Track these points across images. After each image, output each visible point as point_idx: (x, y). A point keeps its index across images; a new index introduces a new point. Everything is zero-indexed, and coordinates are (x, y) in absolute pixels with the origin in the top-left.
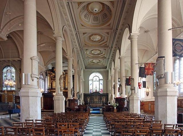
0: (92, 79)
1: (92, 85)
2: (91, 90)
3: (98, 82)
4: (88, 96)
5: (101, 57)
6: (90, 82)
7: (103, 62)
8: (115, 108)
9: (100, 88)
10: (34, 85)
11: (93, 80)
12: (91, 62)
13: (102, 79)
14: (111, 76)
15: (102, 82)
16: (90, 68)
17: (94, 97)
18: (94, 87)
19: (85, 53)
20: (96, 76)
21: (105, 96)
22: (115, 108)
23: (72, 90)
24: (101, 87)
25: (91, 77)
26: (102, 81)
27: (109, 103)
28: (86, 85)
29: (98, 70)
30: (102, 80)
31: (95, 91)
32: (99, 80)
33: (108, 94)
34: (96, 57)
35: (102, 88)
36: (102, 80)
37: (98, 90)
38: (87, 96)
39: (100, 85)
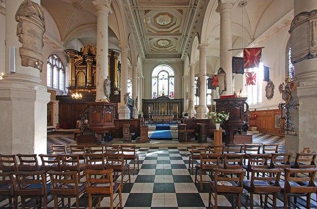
0: (157, 75)
1: (156, 84)
2: (155, 93)
4: (151, 103)
5: (172, 32)
6: (154, 81)
7: (176, 46)
8: (218, 126)
9: (170, 91)
10: (33, 77)
11: (158, 77)
12: (154, 45)
13: (173, 75)
14: (189, 66)
15: (172, 80)
16: (153, 57)
17: (159, 105)
18: (160, 89)
19: (144, 20)
20: (163, 71)
21: (178, 103)
22: (218, 126)
23: (105, 83)
24: (172, 89)
25: (155, 72)
26: (173, 78)
27: (186, 115)
28: (147, 84)
29: (166, 60)
30: (173, 77)
31: (161, 95)
32: (169, 77)
33: (183, 99)
34: (163, 31)
35: (173, 91)
36: (173, 77)
37: (166, 94)
38: (148, 103)
39: (170, 85)
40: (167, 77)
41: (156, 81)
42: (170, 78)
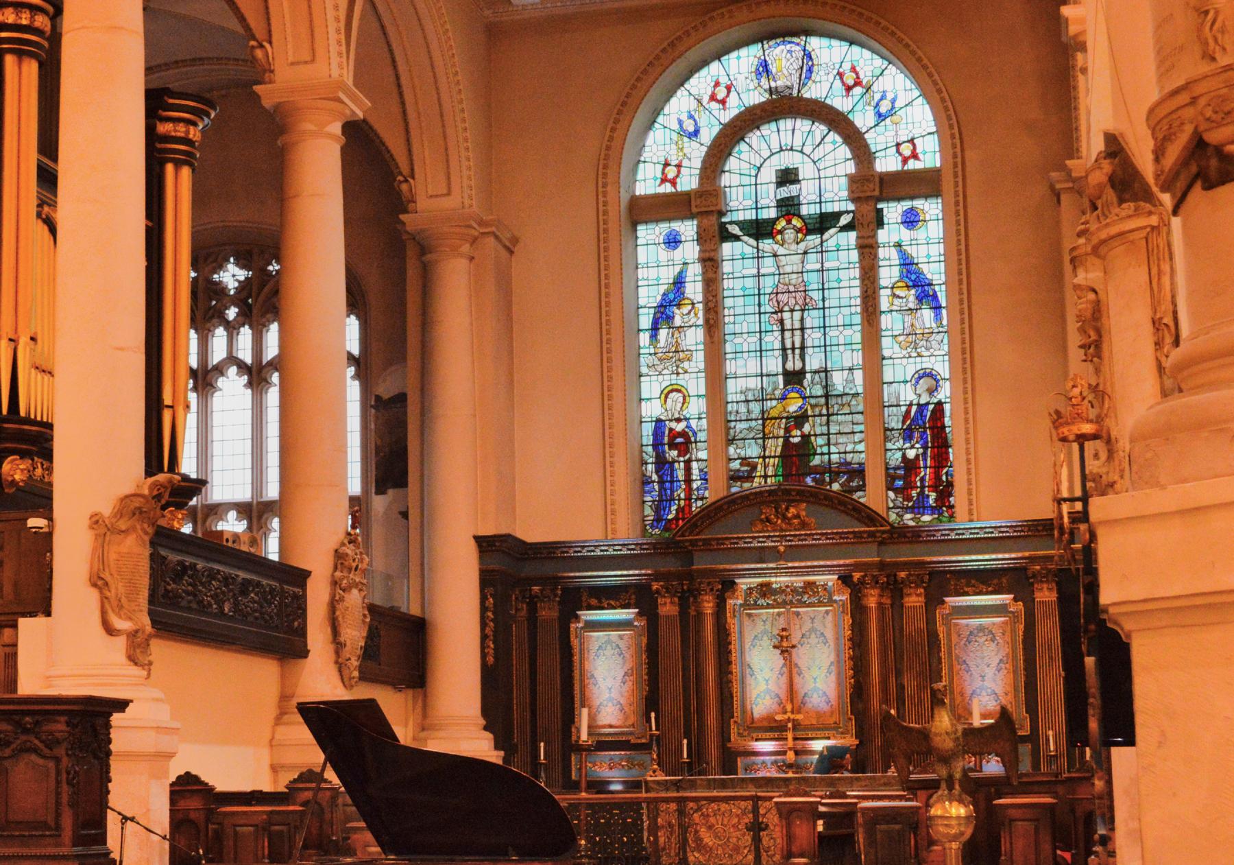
0: (689, 182)
3: (844, 243)
13: (930, 156)
26: (931, 209)
31: (768, 476)
40: (837, 197)
41: (690, 250)
42: (893, 211)
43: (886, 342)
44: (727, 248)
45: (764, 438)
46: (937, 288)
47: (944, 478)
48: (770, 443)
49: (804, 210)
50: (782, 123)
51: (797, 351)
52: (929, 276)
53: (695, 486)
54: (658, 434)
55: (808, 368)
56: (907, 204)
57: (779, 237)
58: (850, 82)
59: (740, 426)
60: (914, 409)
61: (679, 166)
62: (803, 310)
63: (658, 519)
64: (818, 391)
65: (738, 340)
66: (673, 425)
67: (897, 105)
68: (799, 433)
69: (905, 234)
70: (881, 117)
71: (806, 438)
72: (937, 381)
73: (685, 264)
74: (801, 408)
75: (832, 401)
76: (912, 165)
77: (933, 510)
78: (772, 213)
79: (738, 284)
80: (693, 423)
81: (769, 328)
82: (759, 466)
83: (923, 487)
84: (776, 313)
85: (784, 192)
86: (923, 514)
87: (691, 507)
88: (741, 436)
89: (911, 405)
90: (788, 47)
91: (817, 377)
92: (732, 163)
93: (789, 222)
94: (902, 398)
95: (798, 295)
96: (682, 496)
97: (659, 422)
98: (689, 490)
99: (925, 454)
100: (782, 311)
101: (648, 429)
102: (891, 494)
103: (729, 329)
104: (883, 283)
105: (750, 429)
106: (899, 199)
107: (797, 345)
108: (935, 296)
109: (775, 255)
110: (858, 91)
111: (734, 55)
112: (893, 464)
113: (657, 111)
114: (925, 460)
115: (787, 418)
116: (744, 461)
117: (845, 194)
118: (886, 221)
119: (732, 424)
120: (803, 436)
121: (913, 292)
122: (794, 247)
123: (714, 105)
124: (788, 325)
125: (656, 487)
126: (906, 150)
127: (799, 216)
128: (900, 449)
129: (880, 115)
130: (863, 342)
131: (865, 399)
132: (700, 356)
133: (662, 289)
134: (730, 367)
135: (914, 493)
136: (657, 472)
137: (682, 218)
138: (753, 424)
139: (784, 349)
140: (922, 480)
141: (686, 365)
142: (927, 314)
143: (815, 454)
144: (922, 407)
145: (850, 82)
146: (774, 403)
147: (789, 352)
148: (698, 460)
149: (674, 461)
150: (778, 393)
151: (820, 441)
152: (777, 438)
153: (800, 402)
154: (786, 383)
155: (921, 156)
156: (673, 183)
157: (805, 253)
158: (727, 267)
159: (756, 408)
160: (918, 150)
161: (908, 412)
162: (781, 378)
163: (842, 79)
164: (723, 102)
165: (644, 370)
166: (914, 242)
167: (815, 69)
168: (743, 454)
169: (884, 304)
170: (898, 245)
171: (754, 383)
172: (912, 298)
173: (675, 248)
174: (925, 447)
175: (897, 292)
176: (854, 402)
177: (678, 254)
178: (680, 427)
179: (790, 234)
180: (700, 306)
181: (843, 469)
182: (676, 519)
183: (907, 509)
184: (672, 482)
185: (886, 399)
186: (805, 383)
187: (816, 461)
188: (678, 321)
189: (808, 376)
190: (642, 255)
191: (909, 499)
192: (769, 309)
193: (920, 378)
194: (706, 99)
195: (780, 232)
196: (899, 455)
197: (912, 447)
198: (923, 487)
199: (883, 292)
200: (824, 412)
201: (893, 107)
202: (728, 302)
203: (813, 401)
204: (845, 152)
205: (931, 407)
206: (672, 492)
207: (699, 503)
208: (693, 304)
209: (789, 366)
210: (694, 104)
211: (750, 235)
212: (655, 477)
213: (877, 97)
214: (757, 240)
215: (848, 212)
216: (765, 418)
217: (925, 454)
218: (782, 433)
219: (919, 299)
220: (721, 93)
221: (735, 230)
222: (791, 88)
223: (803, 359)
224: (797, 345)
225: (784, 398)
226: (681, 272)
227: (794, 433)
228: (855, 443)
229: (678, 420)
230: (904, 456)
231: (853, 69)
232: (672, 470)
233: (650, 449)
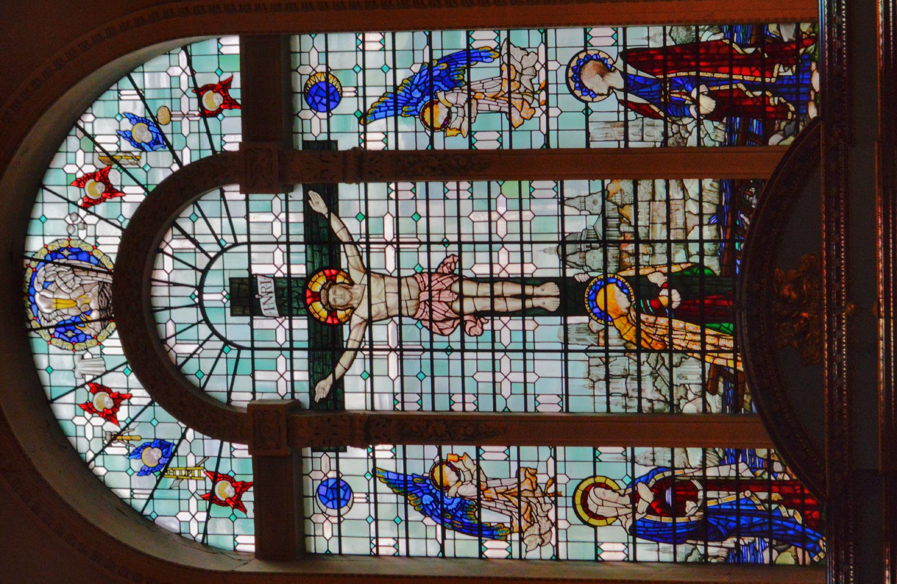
43: (521, 142)
44: (354, 402)
45: (671, 351)
46: (437, 55)
47: (750, 51)
48: (679, 342)
49: (299, 270)
50: (160, 302)
51: (529, 290)
52: (416, 68)
53: (746, 473)
54: (655, 534)
55: (556, 273)
56: (300, 102)
57: (341, 314)
58: (100, 188)
59: (649, 391)
60: (632, 98)
61: (216, 477)
62: (461, 279)
63: (800, 540)
64: (595, 258)
65: (506, 389)
66: (642, 506)
67: (139, 111)
68: (664, 292)
69: (349, 105)
70: (160, 141)
71: (673, 281)
72: (589, 58)
73: (374, 473)
74: (622, 288)
75: (614, 234)
76: (235, 93)
77: (804, 72)
78: (300, 324)
79: (412, 384)
80: (641, 471)
81: (487, 336)
82: (718, 362)
83: (763, 86)
84: (463, 324)
85: (268, 303)
86: (811, 87)
87: (783, 482)
88: (665, 390)
89: (625, 103)
90: (38, 288)
91: (571, 258)
92: (217, 386)
93: (316, 297)
94: (614, 117)
95: (436, 286)
96: (763, 495)
97: (636, 531)
98: (755, 484)
99: (709, 82)
100: (461, 314)
101: (647, 551)
102: (774, 140)
103: (486, 406)
104: (423, 143)
105: (655, 374)
106: (292, 115)
107: (517, 290)
108: (450, 60)
109: (369, 322)
110: (114, 177)
111: (45, 377)
112: (721, 136)
113: (124, 507)
114: (719, 82)
115: (639, 311)
116: (708, 387)
117: (277, 203)
118: (324, 137)
119: (646, 405)
120: (669, 286)
121: (441, 95)
122: (357, 290)
123: (122, 414)
124: (484, 305)
125: (747, 540)
126: (213, 100)
127: (308, 278)
128: (699, 124)
129: (155, 142)
130: (520, 178)
131: (614, 177)
132: (528, 452)
133: (415, 515)
134: (550, 406)
135: (774, 101)
136: (722, 538)
137: (301, 475)
138: (646, 369)
139: (524, 313)
140: (751, 86)
141: (542, 479)
142: (479, 73)
143: (701, 265)
144: (631, 84)
145: (100, 188)
146: (612, 332)
147: (528, 304)
148: (704, 467)
149: (704, 507)
150: (596, 326)
151: (679, 256)
152: (671, 329)
153: (613, 289)
154: (580, 311)
155: (224, 78)
156: (241, 488)
157: (368, 271)
158: (384, 403)
159: (620, 364)
160: (215, 81)
161: (637, 108)
162: (571, 320)
163: (95, 202)
164: (118, 399)
165: (547, 552)
166: (361, 93)
167: (75, 244)
168: (696, 389)
169: (459, 143)
170: (364, 118)
171: (578, 367)
172: (452, 97)
173: (348, 489)
174: (697, 82)
175: (439, 121)
176: (618, 199)
177: (360, 486)
178: (646, 494)
179: (337, 296)
180: (446, 449)
181: (728, 219)
182: (801, 509)
183: (801, 112)
184: (739, 513)
185: (615, 145)
186: (583, 278)
187: (712, 264)
188: (469, 491)
189: (570, 273)
190: (357, 545)
191: (781, 111)
192: (456, 336)
193: (582, 87)
194: (111, 427)
195: (332, 312)
196: (708, 125)
197: (696, 102)
198: (763, 86)
199: (439, 145)
200: (631, 248)
201: (143, 120)
202: (442, 405)
203: (612, 268)
204: (210, 203)
205: (631, 70)
206: (757, 513)
207: (777, 467)
208: (442, 463)
209: (552, 304)
210: (118, 449)
211: (335, 362)
212: (730, 543)
213: (126, 145)
214: (343, 350)
215: (306, 199)
216: (634, 348)
217: (709, 82)
218: (663, 321)
219: (452, 85)
220: (104, 401)
221: (324, 387)
222: (103, 285)
223: (544, 281)
224: (517, 290)
225: (604, 316)
226: (389, 483)
227: (664, 300)
228: (685, 199)
229: (635, 498)
230: (711, 117)
231: (80, 183)
232: (719, 511)
233: (682, 549)
